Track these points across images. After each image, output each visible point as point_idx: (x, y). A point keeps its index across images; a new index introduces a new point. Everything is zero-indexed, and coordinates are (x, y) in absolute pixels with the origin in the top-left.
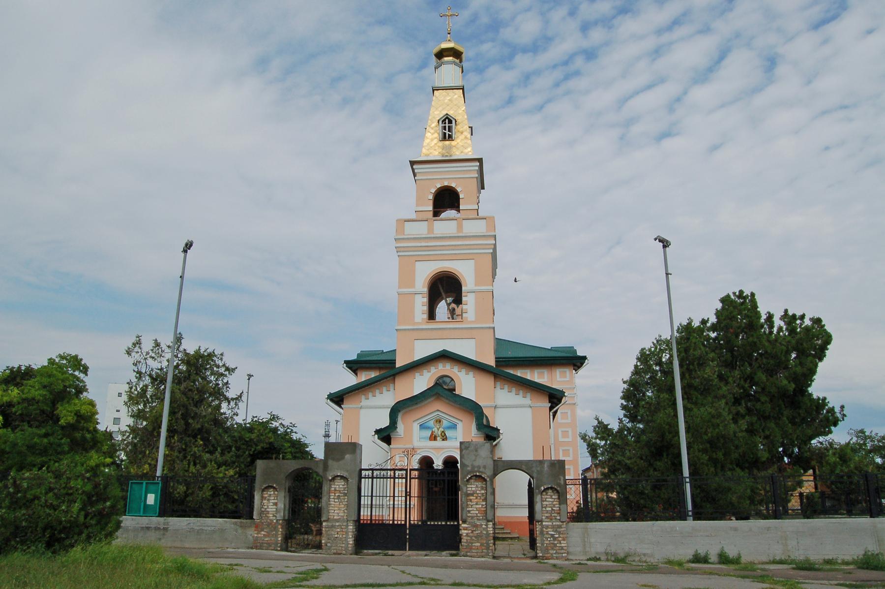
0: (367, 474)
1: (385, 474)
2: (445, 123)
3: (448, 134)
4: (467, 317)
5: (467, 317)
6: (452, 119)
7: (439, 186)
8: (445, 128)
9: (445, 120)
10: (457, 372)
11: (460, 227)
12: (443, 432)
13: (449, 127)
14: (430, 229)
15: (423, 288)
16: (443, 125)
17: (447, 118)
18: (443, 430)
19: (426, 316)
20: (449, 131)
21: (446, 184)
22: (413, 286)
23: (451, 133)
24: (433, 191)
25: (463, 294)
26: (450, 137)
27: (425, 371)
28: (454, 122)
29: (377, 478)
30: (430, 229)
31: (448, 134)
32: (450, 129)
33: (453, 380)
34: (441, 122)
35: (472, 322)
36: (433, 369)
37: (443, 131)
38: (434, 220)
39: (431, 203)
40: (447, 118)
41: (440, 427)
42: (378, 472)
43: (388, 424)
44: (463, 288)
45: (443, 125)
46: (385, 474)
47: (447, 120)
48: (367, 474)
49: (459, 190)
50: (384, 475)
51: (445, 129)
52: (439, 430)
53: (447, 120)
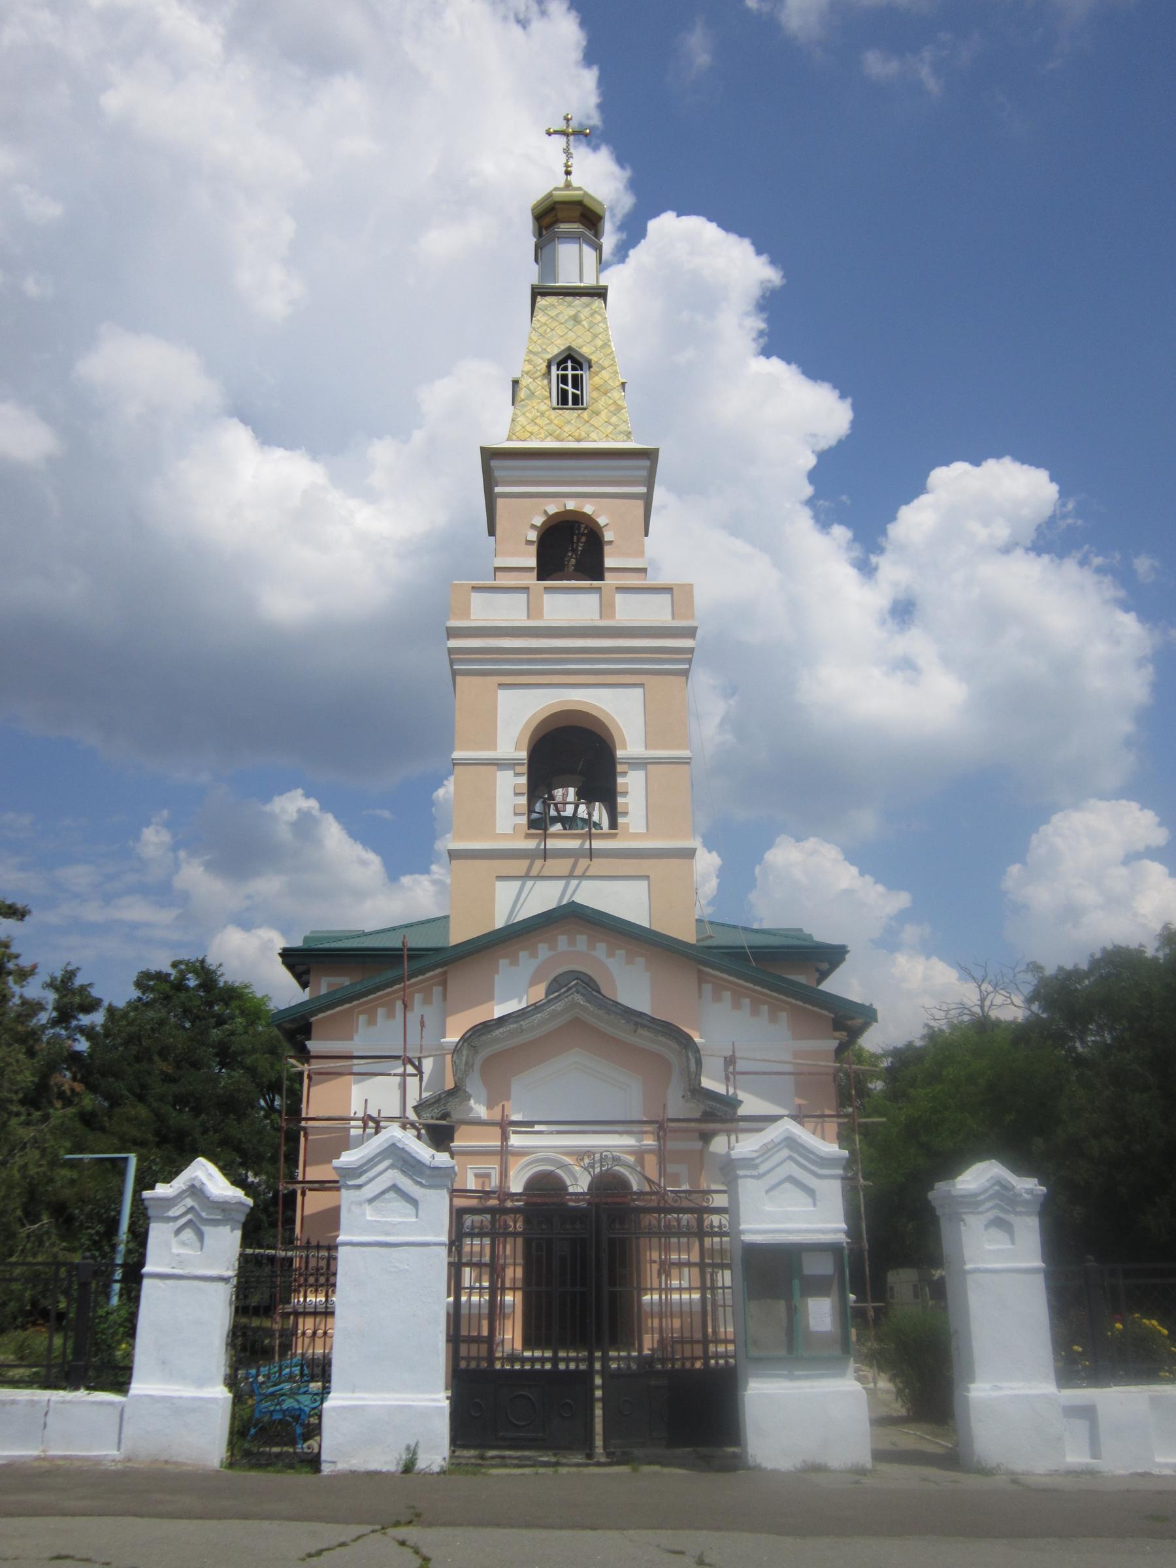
2: (565, 369)
3: (573, 394)
4: (627, 824)
5: (627, 824)
7: (553, 508)
8: (563, 379)
9: (564, 361)
11: (606, 608)
13: (575, 377)
14: (533, 609)
16: (560, 372)
20: (575, 386)
21: (571, 505)
22: (495, 749)
23: (579, 392)
24: (539, 521)
25: (619, 768)
26: (577, 400)
27: (523, 955)
30: (533, 609)
31: (573, 394)
32: (577, 382)
34: (554, 368)
35: (636, 836)
39: (533, 549)
44: (620, 753)
45: (560, 372)
49: (602, 521)
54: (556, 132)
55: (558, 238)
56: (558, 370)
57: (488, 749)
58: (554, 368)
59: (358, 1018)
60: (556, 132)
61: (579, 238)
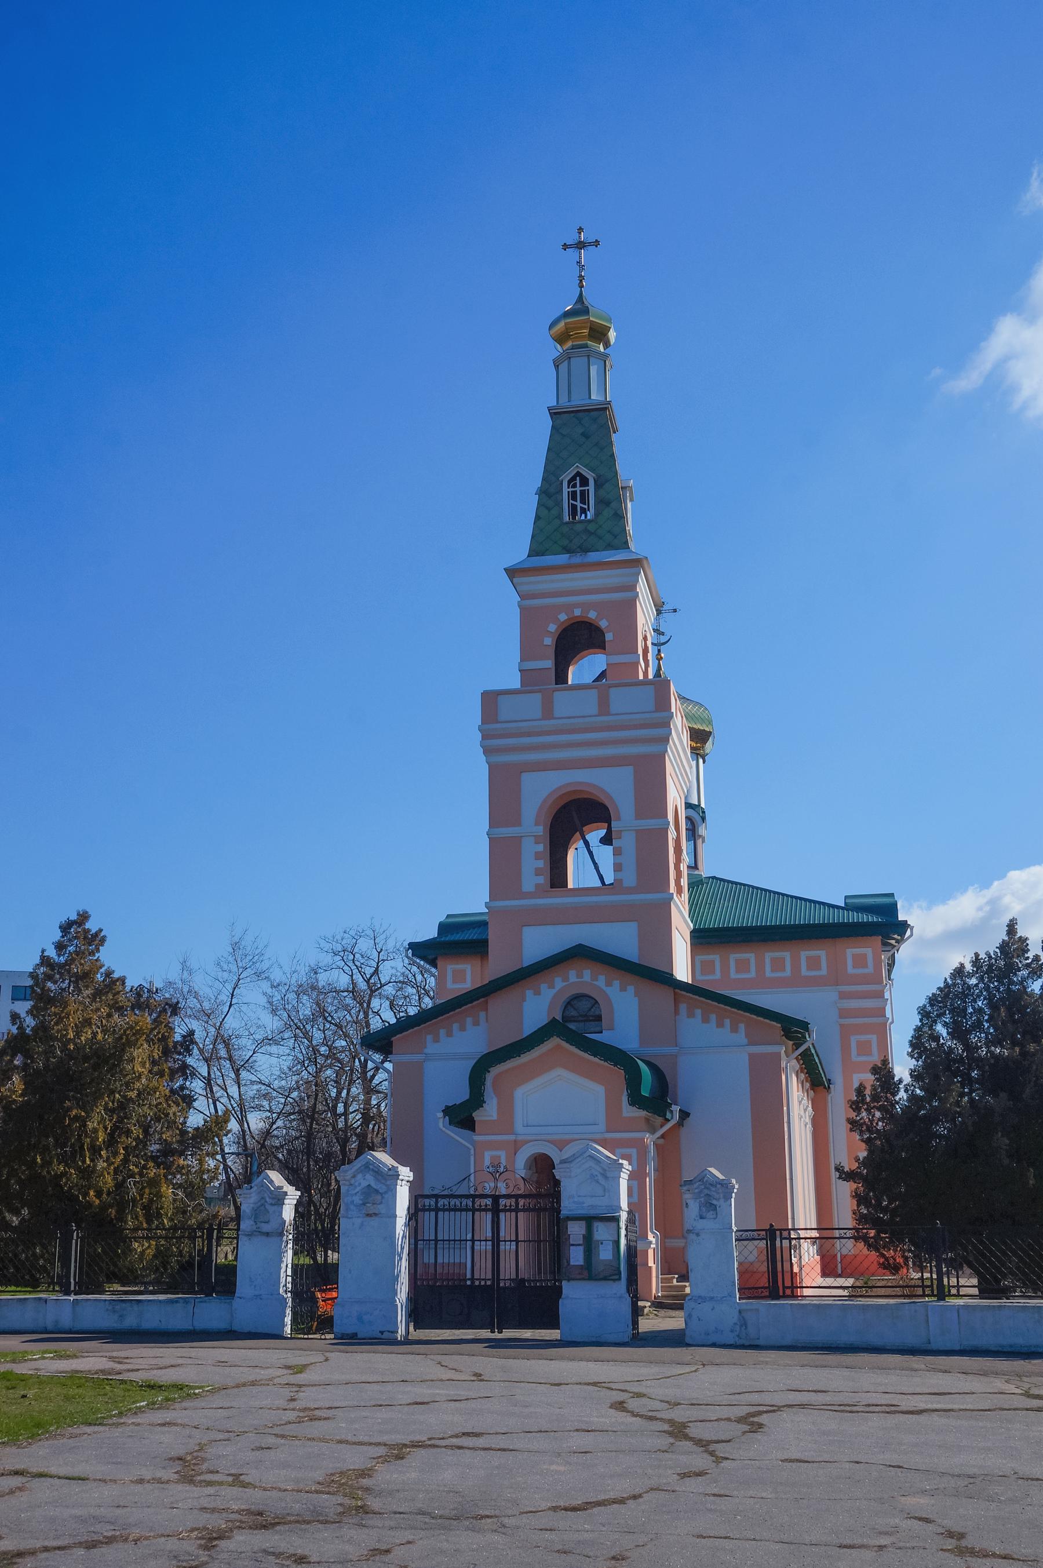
0: (427, 1204)
1: (458, 1203)
2: (574, 486)
8: (573, 496)
9: (573, 479)
10: (604, 988)
13: (582, 493)
15: (537, 824)
16: (571, 490)
19: (543, 880)
20: (583, 501)
21: (577, 612)
28: (591, 482)
29: (444, 1210)
33: (597, 1002)
34: (565, 484)
36: (559, 983)
37: (571, 501)
40: (578, 474)
42: (446, 1201)
43: (467, 1097)
45: (571, 490)
46: (458, 1203)
47: (578, 478)
48: (427, 1204)
50: (455, 1206)
51: (574, 498)
53: (578, 478)
56: (568, 488)
57: (514, 825)
59: (426, 1038)
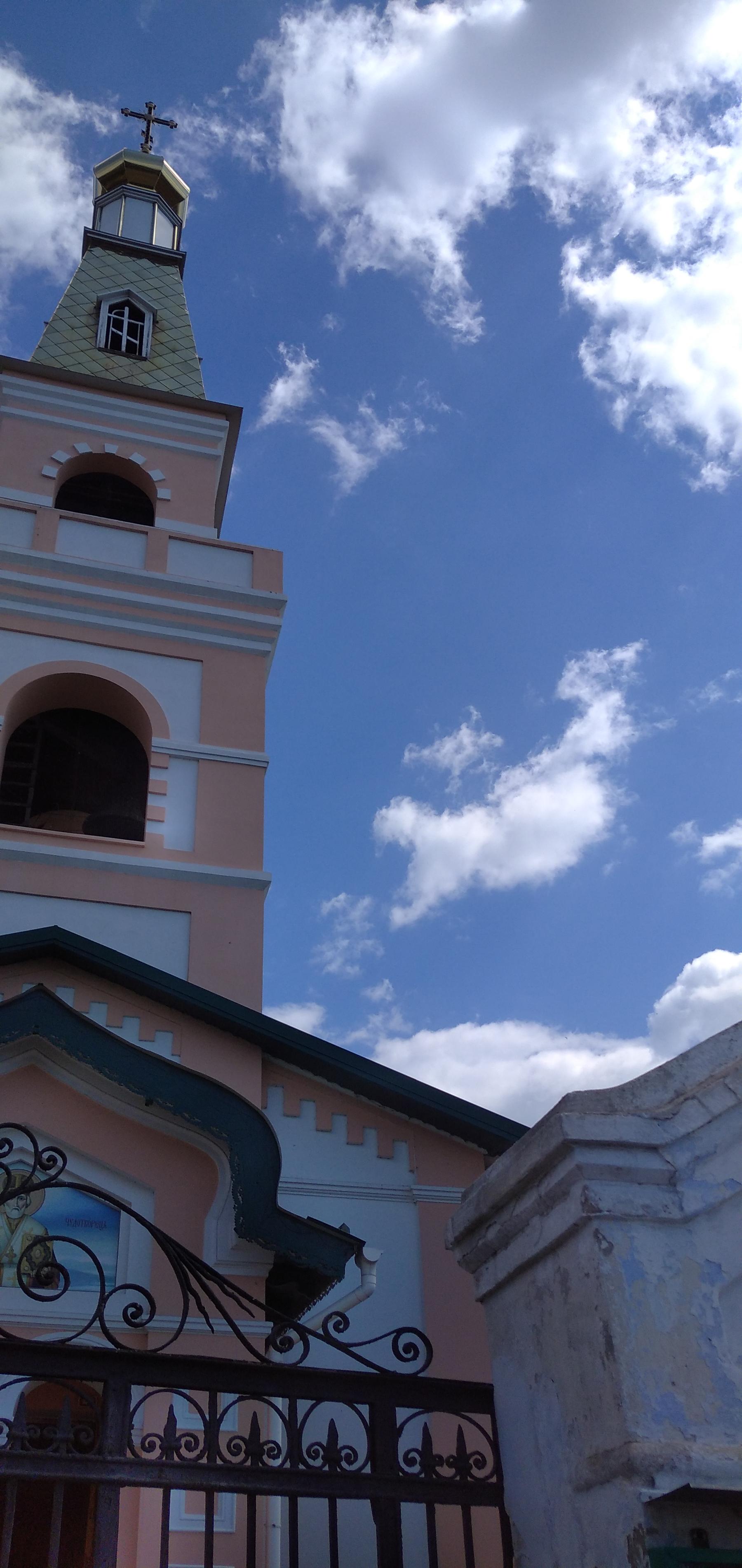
6: (143, 309)
7: (84, 448)
12: (39, 1241)
17: (127, 303)
18: (38, 1231)
21: (112, 449)
24: (63, 457)
34: (105, 308)
37: (112, 328)
38: (61, 517)
41: (23, 1217)
47: (127, 309)
52: (21, 1226)
53: (127, 309)
54: (133, 114)
55: (126, 196)
58: (105, 308)
60: (133, 114)
61: (154, 204)
